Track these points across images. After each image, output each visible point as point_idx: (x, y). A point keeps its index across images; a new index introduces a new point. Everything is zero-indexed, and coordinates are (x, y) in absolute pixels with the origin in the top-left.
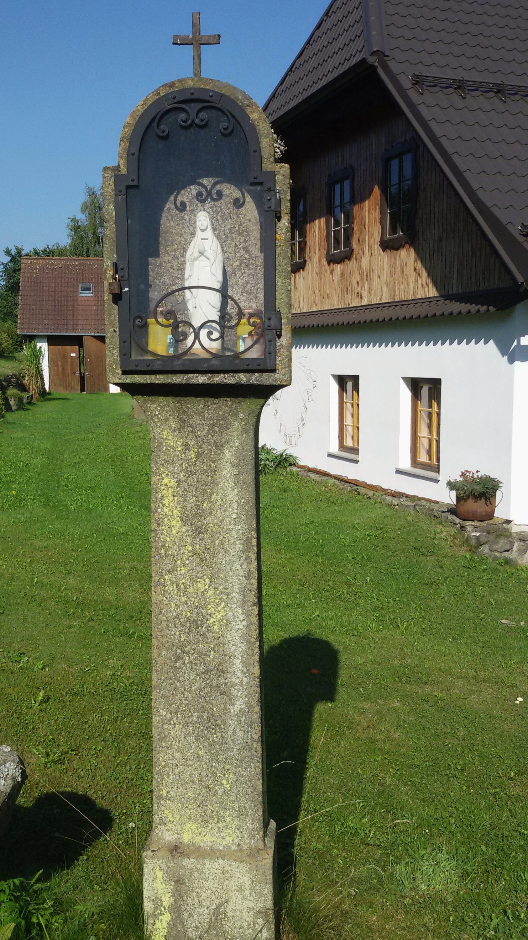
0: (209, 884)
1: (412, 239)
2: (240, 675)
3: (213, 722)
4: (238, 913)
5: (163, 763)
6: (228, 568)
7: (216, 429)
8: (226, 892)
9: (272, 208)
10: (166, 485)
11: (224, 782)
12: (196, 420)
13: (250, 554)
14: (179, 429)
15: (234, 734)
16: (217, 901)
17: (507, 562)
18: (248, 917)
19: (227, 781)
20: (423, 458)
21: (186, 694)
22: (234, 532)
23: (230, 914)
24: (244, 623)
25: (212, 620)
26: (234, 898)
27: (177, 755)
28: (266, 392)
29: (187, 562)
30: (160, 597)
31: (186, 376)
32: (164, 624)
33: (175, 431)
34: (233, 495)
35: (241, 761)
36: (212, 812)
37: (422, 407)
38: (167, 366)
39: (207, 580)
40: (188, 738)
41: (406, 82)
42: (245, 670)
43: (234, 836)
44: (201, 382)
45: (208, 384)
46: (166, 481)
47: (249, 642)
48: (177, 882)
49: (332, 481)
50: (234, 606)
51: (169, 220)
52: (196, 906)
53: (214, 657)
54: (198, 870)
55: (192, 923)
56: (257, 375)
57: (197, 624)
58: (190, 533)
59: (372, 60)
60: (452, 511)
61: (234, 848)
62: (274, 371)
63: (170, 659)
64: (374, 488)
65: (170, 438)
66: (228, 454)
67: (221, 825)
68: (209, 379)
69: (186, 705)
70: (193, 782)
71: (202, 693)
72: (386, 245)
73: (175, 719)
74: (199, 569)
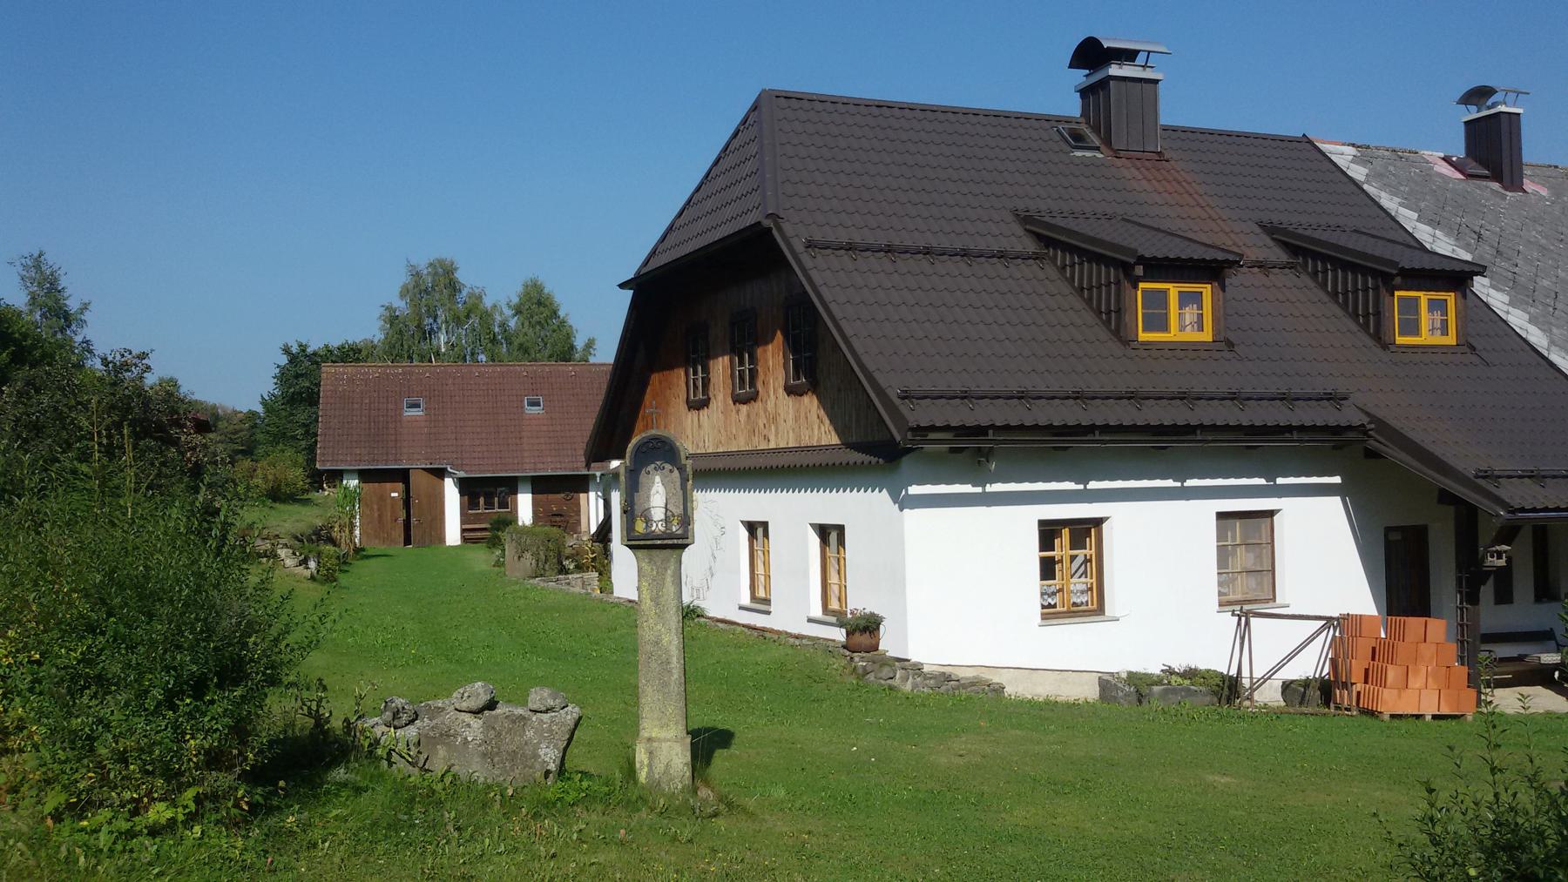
1: (814, 387)
3: (665, 684)
17: (891, 688)
20: (834, 605)
28: (684, 546)
37: (831, 552)
38: (645, 537)
41: (799, 246)
49: (739, 629)
51: (643, 477)
55: (656, 771)
59: (767, 223)
60: (844, 647)
64: (778, 633)
72: (790, 391)
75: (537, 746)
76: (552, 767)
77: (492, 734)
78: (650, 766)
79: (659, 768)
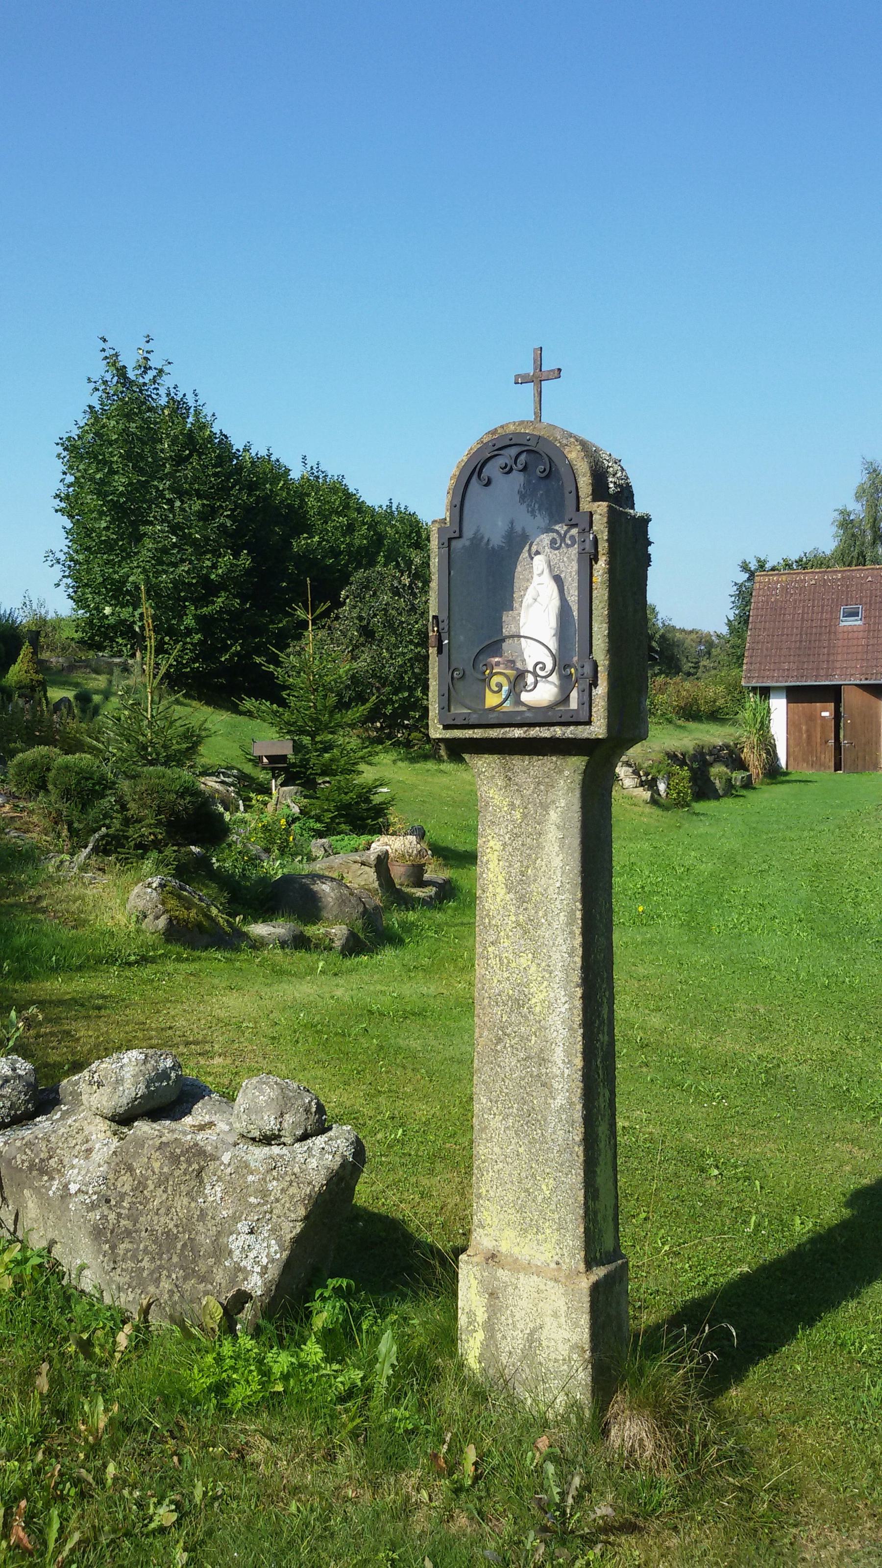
0: (523, 1303)
2: (562, 1066)
4: (553, 1343)
5: (483, 1158)
6: (551, 942)
7: (542, 787)
8: (540, 1315)
9: (586, 550)
10: (491, 848)
11: (544, 1187)
12: (521, 778)
13: (574, 928)
14: (505, 787)
15: (554, 1133)
16: (531, 1325)
18: (564, 1350)
19: (547, 1186)
21: (507, 1081)
22: (557, 902)
23: (544, 1343)
24: (567, 1006)
25: (533, 1001)
26: (549, 1324)
27: (497, 1149)
29: (511, 934)
30: (483, 971)
31: (503, 730)
32: (486, 1001)
33: (501, 789)
34: (557, 862)
35: (562, 1165)
36: (531, 1220)
39: (530, 956)
40: (508, 1132)
42: (566, 1061)
43: (554, 1252)
44: (517, 736)
45: (524, 738)
46: (491, 843)
47: (571, 1029)
48: (491, 1294)
50: (556, 986)
52: (510, 1327)
53: (536, 1042)
54: (512, 1284)
55: (505, 1346)
56: (572, 728)
57: (519, 1003)
58: (514, 902)
61: (553, 1265)
62: (589, 723)
63: (492, 1041)
65: (496, 797)
66: (554, 816)
67: (540, 1237)
68: (525, 733)
69: (507, 1094)
70: (512, 1182)
71: (523, 1083)
73: (495, 1108)
74: (522, 942)
75: (226, 1229)
76: (255, 1284)
77: (126, 1183)
78: (490, 1327)
79: (512, 1342)
